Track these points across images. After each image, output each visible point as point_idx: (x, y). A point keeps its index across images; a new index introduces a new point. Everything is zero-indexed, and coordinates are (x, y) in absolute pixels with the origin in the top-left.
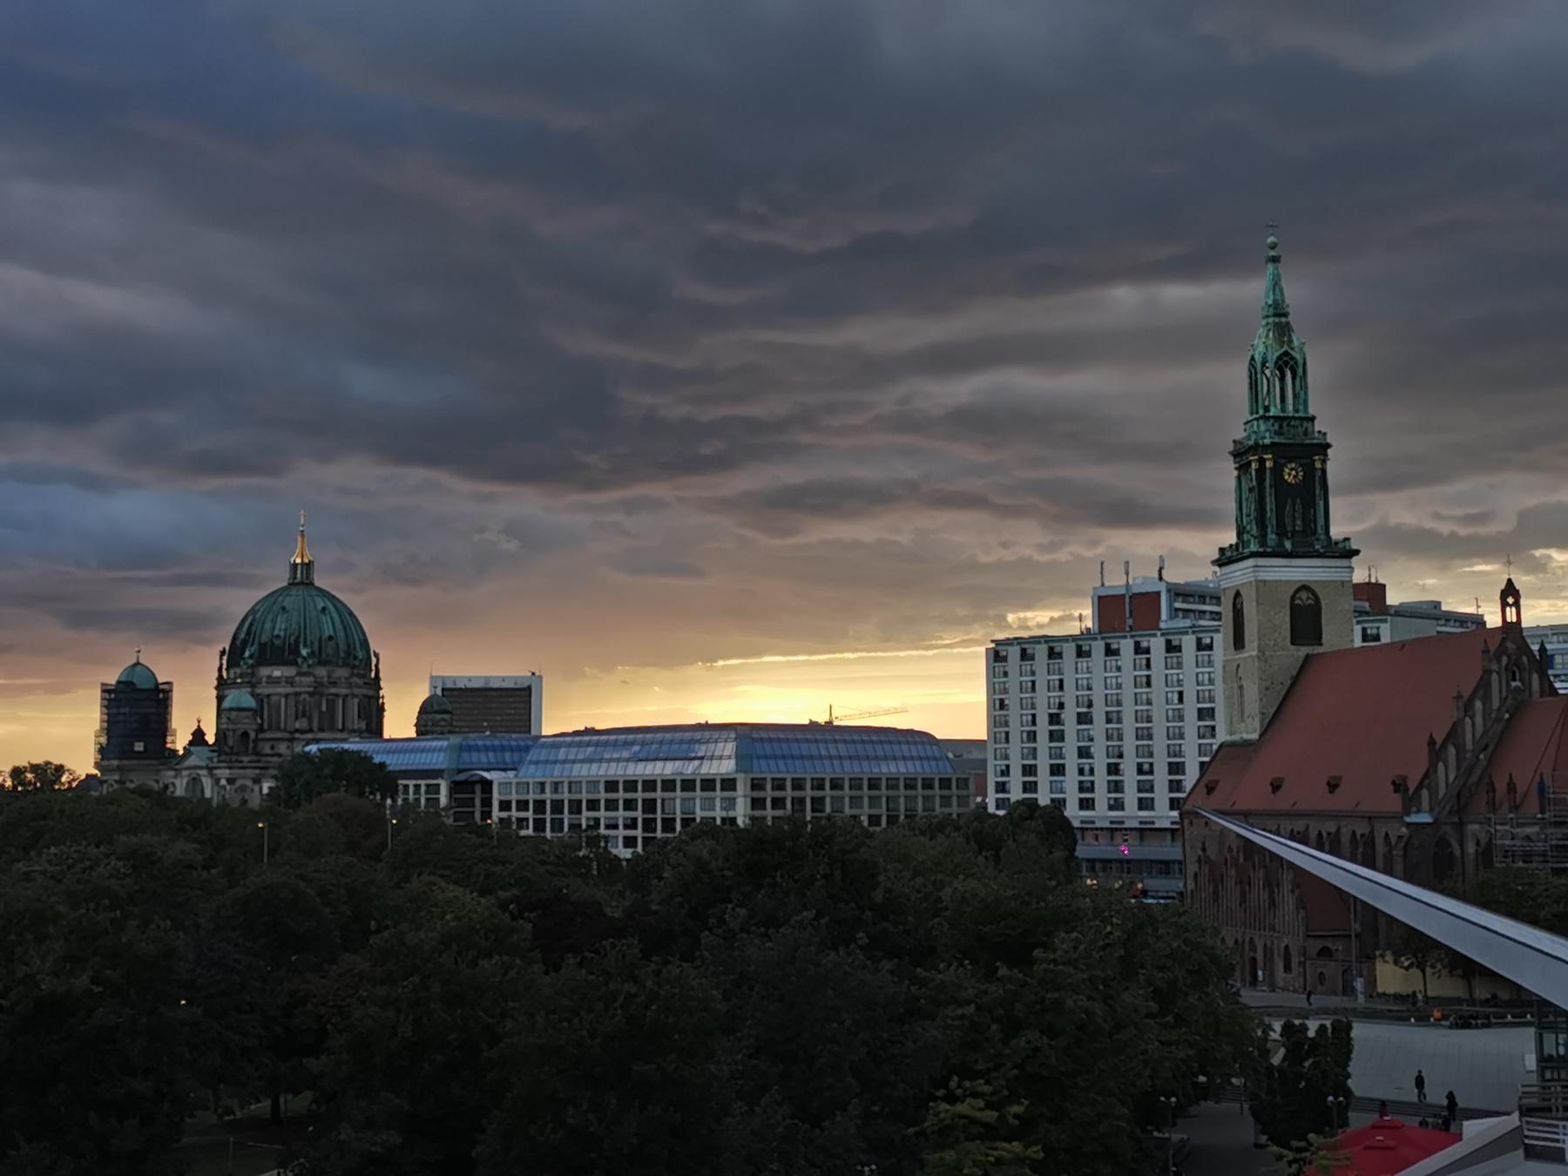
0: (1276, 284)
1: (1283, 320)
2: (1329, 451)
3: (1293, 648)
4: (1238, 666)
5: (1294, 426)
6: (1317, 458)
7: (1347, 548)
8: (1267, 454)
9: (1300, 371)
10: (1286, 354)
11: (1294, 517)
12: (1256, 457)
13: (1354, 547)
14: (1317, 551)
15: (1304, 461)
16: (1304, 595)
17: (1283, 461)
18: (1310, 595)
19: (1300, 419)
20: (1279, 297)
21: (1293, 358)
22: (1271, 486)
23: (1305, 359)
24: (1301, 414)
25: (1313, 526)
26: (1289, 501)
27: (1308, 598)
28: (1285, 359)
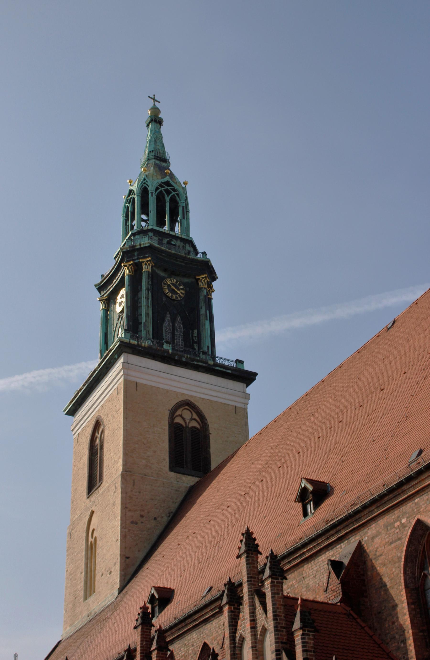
0: (157, 138)
1: (164, 164)
2: (214, 284)
3: (172, 474)
4: (93, 512)
5: (175, 245)
6: (201, 277)
7: (240, 366)
8: (144, 258)
9: (182, 204)
10: (167, 183)
11: (173, 333)
12: (131, 262)
13: (248, 367)
14: (206, 363)
15: (186, 280)
16: (187, 414)
17: (162, 274)
18: (195, 416)
19: (182, 240)
20: (160, 148)
21: (174, 190)
22: (148, 289)
23: (186, 197)
24: (183, 237)
25: (196, 347)
26: (168, 317)
27: (192, 419)
28: (166, 187)
